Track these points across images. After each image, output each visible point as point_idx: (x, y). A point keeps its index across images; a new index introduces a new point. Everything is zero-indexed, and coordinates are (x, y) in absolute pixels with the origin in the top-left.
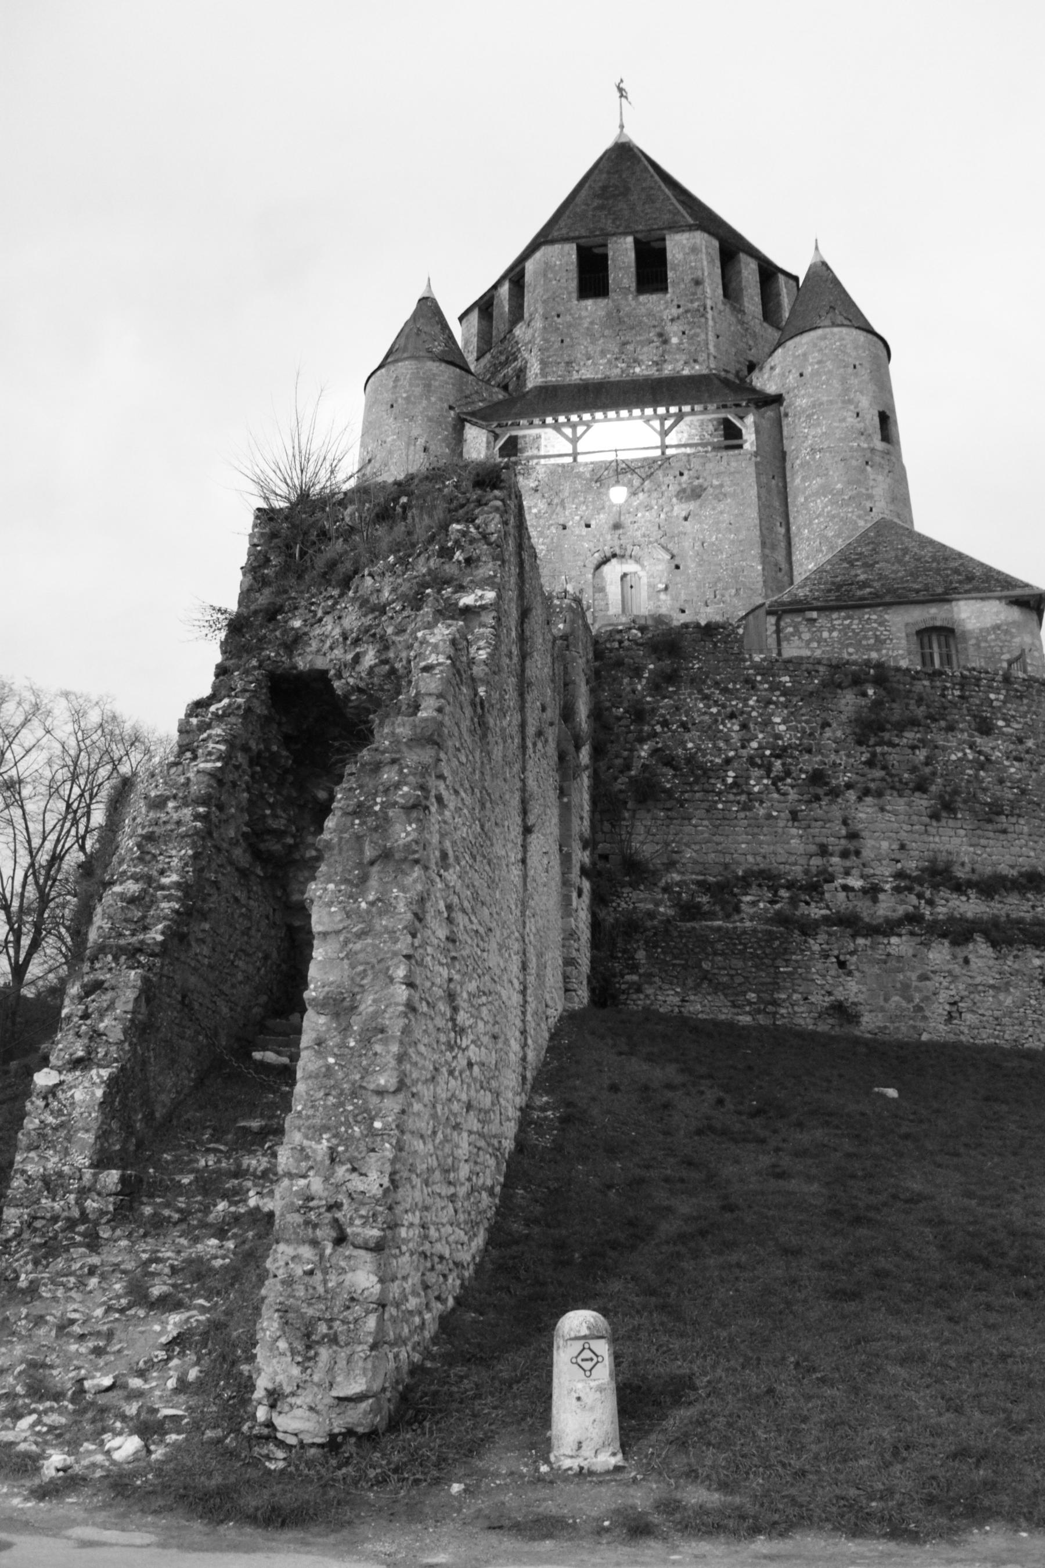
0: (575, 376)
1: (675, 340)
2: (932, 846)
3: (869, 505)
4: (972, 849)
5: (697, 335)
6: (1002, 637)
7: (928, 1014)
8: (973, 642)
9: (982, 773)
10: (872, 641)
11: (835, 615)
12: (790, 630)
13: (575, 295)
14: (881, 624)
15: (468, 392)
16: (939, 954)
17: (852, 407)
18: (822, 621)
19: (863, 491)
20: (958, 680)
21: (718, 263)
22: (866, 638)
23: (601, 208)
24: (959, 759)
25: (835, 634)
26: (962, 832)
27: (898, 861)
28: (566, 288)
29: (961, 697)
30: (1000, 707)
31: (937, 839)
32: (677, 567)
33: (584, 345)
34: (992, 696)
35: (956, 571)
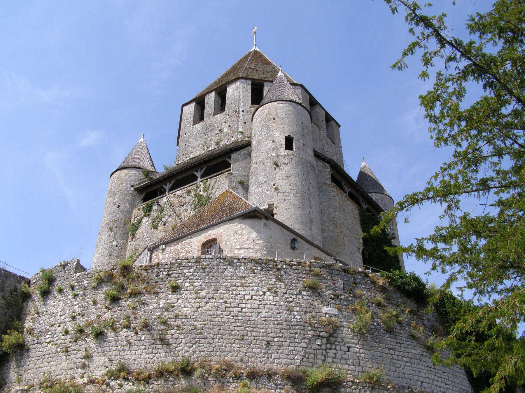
0: (188, 158)
1: (225, 130)
4: (148, 355)
6: (238, 237)
13: (192, 124)
18: (168, 249)
20: (168, 266)
25: (171, 255)
29: (166, 275)
30: (190, 276)
31: (128, 353)
34: (186, 271)
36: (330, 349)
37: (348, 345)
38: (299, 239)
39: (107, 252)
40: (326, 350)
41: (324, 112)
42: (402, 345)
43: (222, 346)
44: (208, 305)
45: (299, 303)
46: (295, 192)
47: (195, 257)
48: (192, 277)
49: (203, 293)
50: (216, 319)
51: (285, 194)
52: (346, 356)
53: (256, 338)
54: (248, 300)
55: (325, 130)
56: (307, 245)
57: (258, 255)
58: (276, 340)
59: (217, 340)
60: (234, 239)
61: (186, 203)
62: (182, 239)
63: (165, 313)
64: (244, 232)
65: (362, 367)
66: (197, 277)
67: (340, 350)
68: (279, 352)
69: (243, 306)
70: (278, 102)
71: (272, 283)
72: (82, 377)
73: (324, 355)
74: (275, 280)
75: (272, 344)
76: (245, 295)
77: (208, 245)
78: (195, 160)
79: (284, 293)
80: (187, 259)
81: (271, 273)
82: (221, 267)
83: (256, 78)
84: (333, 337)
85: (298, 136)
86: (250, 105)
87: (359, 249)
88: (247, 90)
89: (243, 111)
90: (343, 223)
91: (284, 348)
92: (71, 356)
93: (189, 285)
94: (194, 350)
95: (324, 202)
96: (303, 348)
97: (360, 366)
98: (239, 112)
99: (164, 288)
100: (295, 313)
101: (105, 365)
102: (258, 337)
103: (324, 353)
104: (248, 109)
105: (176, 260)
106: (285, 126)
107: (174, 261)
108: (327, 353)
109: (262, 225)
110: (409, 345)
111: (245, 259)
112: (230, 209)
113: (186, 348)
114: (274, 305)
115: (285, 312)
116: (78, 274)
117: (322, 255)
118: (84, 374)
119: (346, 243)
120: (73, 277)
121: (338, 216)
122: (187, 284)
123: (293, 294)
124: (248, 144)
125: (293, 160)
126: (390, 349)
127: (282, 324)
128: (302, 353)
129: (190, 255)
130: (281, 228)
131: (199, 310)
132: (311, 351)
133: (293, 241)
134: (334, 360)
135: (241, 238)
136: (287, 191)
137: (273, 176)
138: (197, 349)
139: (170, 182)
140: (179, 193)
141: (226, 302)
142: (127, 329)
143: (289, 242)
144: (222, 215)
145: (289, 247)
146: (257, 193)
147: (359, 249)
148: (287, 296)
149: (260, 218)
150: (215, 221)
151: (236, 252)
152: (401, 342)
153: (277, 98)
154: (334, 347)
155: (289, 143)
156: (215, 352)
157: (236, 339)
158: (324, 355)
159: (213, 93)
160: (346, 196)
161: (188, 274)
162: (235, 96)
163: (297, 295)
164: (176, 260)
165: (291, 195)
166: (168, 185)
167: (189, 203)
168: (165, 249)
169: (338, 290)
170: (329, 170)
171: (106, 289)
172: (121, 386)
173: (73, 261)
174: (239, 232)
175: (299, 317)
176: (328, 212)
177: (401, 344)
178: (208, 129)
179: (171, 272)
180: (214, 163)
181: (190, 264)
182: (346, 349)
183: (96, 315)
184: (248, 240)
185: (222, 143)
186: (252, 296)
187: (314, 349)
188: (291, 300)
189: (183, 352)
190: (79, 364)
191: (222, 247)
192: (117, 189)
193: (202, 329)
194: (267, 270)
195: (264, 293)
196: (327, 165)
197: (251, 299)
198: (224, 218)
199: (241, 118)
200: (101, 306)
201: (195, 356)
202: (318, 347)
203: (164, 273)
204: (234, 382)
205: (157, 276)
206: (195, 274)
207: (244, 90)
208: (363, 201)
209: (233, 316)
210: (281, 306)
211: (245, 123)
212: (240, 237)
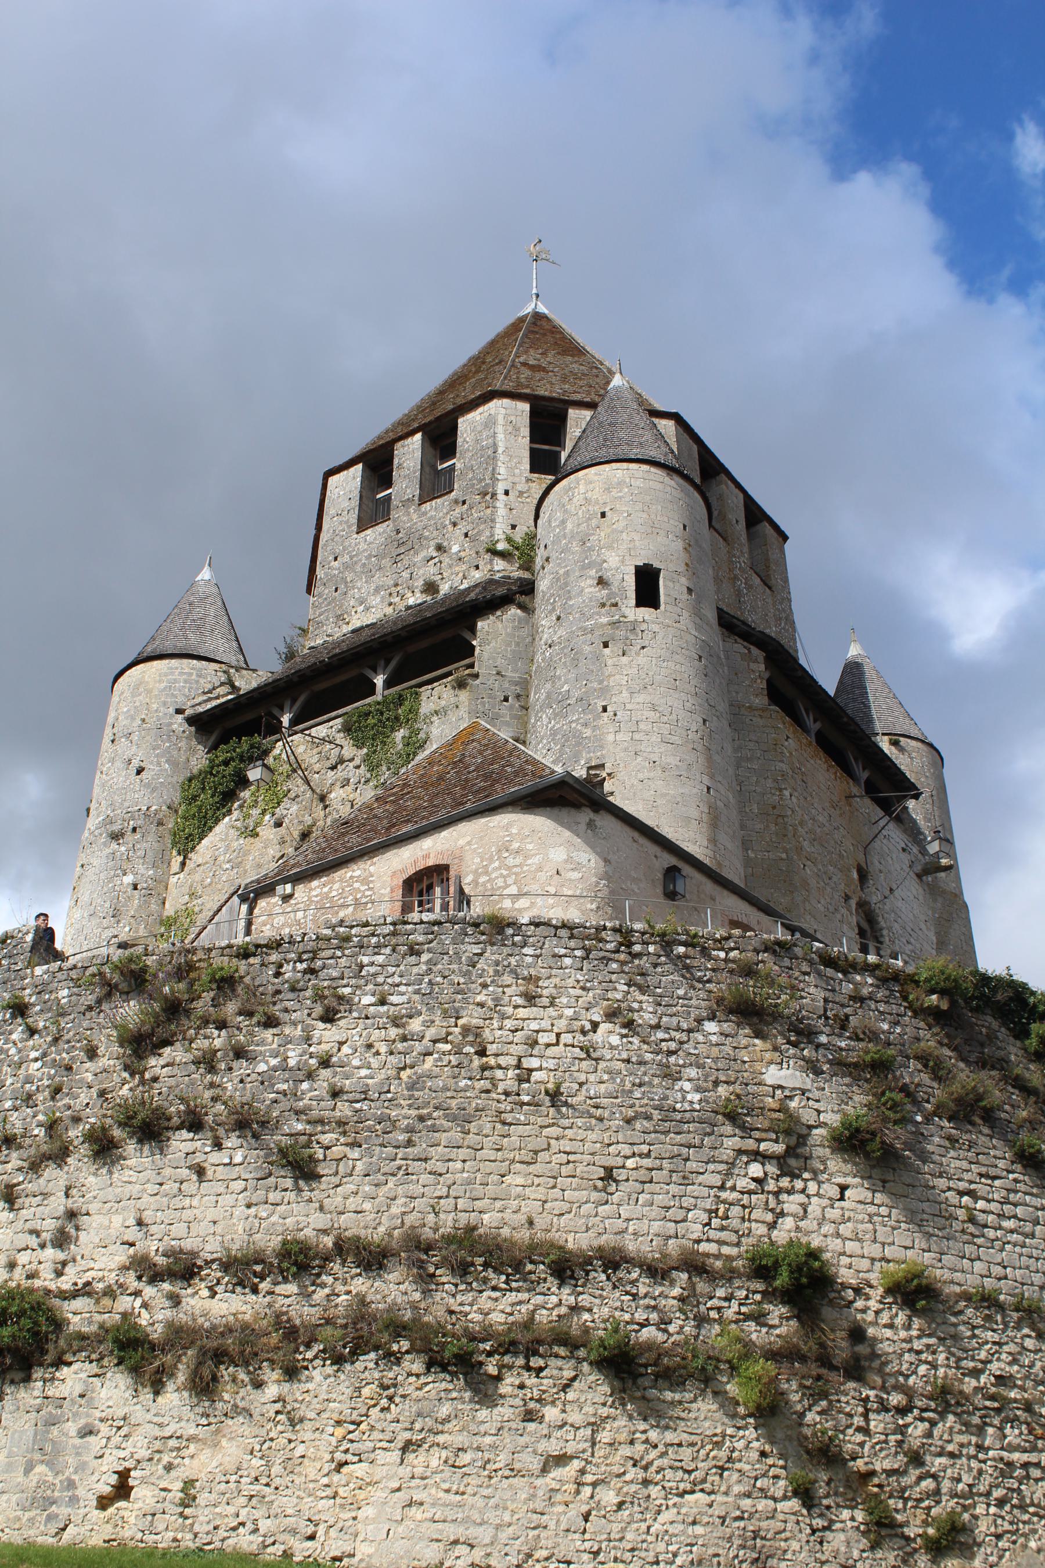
0: (346, 629)
1: (455, 549)
2: (187, 1214)
5: (479, 533)
6: (511, 861)
7: (80, 1492)
11: (315, 883)
13: (355, 528)
15: (209, 686)
16: (115, 1390)
19: (595, 685)
21: (526, 431)
26: (239, 1185)
27: (132, 1245)
28: (347, 522)
30: (375, 975)
31: (195, 1202)
33: (362, 587)
36: (790, 1192)
37: (840, 1180)
38: (687, 869)
39: (107, 905)
40: (776, 1194)
41: (741, 496)
42: (997, 1183)
44: (430, 1060)
45: (697, 1055)
46: (665, 729)
47: (389, 920)
48: (380, 979)
49: (415, 1025)
50: (453, 1103)
52: (833, 1214)
53: (571, 1158)
54: (548, 1045)
55: (746, 549)
56: (709, 886)
57: (574, 915)
58: (630, 1163)
59: (459, 1165)
60: (499, 868)
61: (341, 761)
63: (305, 1086)
64: (530, 847)
65: (883, 1244)
66: (397, 979)
67: (818, 1195)
69: (534, 1063)
70: (614, 465)
71: (619, 996)
72: (59, 1274)
73: (772, 1210)
74: (625, 988)
75: (620, 1174)
76: (537, 1032)
77: (422, 884)
78: (364, 636)
79: (652, 1027)
80: (366, 924)
81: (615, 966)
82: (469, 947)
83: (542, 392)
84: (797, 1156)
85: (672, 567)
86: (527, 474)
87: (847, 898)
88: (517, 430)
89: (507, 493)
90: (802, 823)
91: (656, 1188)
92: (24, 1211)
93: (373, 1000)
94: (391, 1195)
95: (748, 760)
96: (712, 1187)
97: (875, 1241)
98: (494, 495)
99: (300, 1013)
100: (687, 1086)
101: (125, 1239)
102: (577, 1157)
103: (772, 1204)
104: (520, 487)
105: (333, 927)
106: (636, 537)
107: (328, 932)
108: (779, 1202)
109: (583, 827)
110: (1016, 1181)
111: (537, 925)
112: (486, 777)
113: (367, 1188)
114: (623, 1061)
115: (656, 1081)
116: (39, 970)
117: (751, 915)
118: (64, 1264)
119: (813, 882)
120: (23, 979)
121: (788, 802)
122: (367, 1000)
123: (678, 1029)
124: (528, 588)
125: (659, 637)
126: (961, 1193)
127: (648, 1117)
128: (708, 1204)
129: (371, 913)
130: (636, 835)
131: (404, 1075)
132: (735, 1195)
133: (671, 873)
134: (801, 1224)
135: (520, 865)
136: (642, 726)
137: (601, 682)
138: (400, 1190)
139: (294, 701)
140: (321, 731)
142: (189, 1131)
143: (660, 876)
144: (465, 795)
145: (659, 890)
146: (554, 733)
147: (847, 898)
148: (660, 1035)
149: (576, 806)
150: (442, 814)
151: (507, 904)
152: (992, 1172)
153: (612, 453)
154: (799, 1184)
155: (647, 586)
156: (451, 1200)
157: (513, 1161)
158: (772, 1210)
159: (418, 436)
160: (810, 743)
161: (372, 970)
162: (482, 448)
163: (690, 1031)
164: (333, 927)
165: (655, 738)
167: (352, 760)
168: (291, 896)
169: (809, 1018)
170: (762, 667)
171: (130, 1011)
172: (175, 1300)
173: (25, 930)
174: (515, 845)
175: (697, 1097)
176: (758, 789)
177: (994, 1178)
178: (403, 545)
179: (319, 963)
180: (424, 644)
181: (374, 940)
182: (835, 1192)
183: (94, 1092)
184: (540, 869)
185: (444, 588)
186: (558, 1035)
187: (742, 1193)
188: (673, 1046)
189: (359, 1199)
190: (46, 1236)
191: (467, 890)
192: (133, 719)
193: (410, 1130)
194: (604, 958)
195: (595, 1025)
196: (755, 651)
197: (557, 1044)
198: (468, 806)
199: (502, 511)
200: (111, 1062)
201: (395, 1210)
202: (753, 1186)
203: (300, 966)
204: (511, 1290)
205: (277, 974)
206: (391, 970)
207: (510, 429)
208: (856, 759)
209: (507, 1094)
210: (645, 1063)
211: (514, 527)
212: (518, 861)
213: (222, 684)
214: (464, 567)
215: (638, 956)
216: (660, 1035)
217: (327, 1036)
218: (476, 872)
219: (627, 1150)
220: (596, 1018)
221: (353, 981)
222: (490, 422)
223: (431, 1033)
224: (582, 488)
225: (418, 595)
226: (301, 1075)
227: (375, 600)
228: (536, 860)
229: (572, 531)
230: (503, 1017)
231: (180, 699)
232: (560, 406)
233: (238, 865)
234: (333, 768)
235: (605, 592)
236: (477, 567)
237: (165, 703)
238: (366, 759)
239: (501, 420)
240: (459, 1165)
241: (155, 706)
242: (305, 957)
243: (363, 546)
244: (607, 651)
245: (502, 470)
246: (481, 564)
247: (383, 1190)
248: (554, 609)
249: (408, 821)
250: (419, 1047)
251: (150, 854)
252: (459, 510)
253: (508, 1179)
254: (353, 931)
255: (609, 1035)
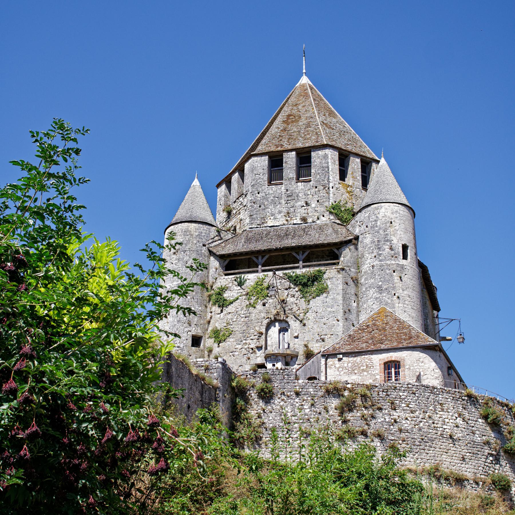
1: (313, 205)
3: (393, 292)
6: (420, 364)
8: (407, 367)
9: (392, 427)
10: (365, 367)
12: (331, 363)
13: (266, 182)
14: (368, 360)
15: (212, 236)
17: (388, 243)
19: (391, 285)
21: (337, 163)
22: (362, 366)
23: (285, 130)
24: (382, 421)
25: (350, 365)
28: (263, 179)
30: (405, 398)
32: (304, 325)
35: (405, 334)
43: (434, 456)
50: (429, 436)
51: (405, 306)
58: (468, 454)
61: (290, 288)
62: (361, 354)
68: (470, 463)
69: (445, 427)
80: (400, 384)
81: (459, 402)
86: (339, 181)
91: (473, 461)
93: (405, 405)
100: (477, 436)
122: (403, 405)
127: (471, 444)
128: (483, 466)
137: (393, 285)
141: (433, 423)
148: (471, 422)
149: (436, 350)
159: (294, 153)
161: (403, 397)
163: (476, 421)
165: (410, 307)
166: (260, 258)
168: (342, 359)
174: (421, 360)
181: (403, 388)
189: (410, 458)
199: (331, 195)
206: (409, 397)
207: (333, 161)
213: (217, 236)
214: (318, 214)
215: (464, 400)
216: (471, 422)
217: (395, 414)
218: (409, 365)
219: (467, 451)
220: (457, 416)
221: (399, 400)
222: (326, 156)
223: (421, 416)
224: (383, 210)
225: (298, 220)
226: (390, 424)
227: (279, 216)
228: (427, 365)
229: (380, 226)
230: (437, 414)
231: (204, 240)
232: (347, 153)
233: (248, 317)
234: (286, 289)
235: (393, 252)
236: (323, 216)
237: (198, 241)
238: (300, 290)
239: (330, 157)
240: (432, 452)
241: (195, 242)
242: (385, 391)
243: (271, 192)
244: (395, 274)
245: (331, 178)
246: (325, 215)
247: (415, 456)
248: (373, 252)
249: (382, 343)
250: (419, 420)
251: (199, 301)
252: (314, 190)
253: (443, 456)
254: (397, 385)
255: (459, 421)
